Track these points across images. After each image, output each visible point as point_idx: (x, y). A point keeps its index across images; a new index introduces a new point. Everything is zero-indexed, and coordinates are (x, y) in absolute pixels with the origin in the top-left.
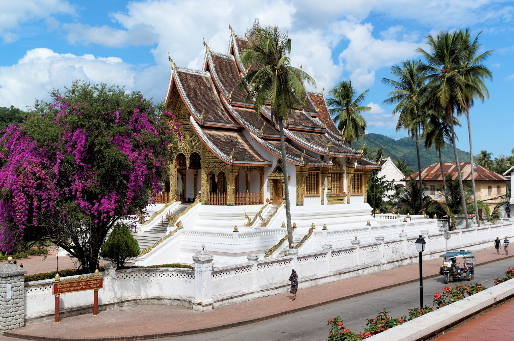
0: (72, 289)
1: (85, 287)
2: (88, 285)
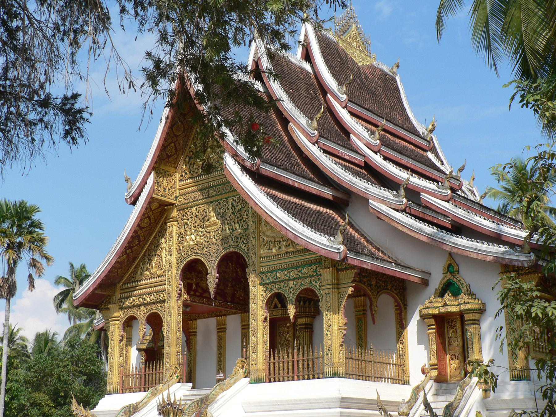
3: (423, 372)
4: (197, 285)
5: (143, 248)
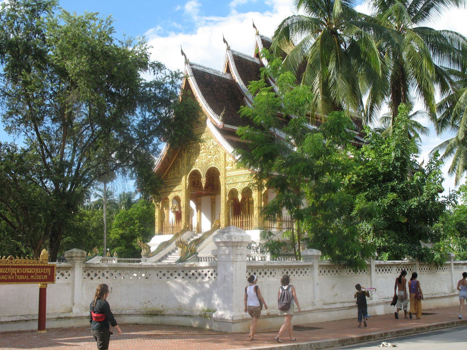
1: (22, 277)
5: (170, 163)
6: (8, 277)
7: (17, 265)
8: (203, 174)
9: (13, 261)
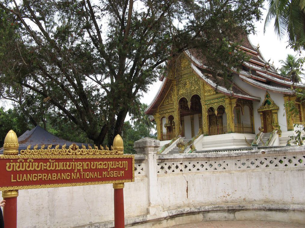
0: (55, 176)
2: (97, 170)
3: (259, 130)
4: (184, 105)
5: (166, 95)
6: (71, 176)
7: (84, 157)
8: (189, 100)
9: (76, 151)
